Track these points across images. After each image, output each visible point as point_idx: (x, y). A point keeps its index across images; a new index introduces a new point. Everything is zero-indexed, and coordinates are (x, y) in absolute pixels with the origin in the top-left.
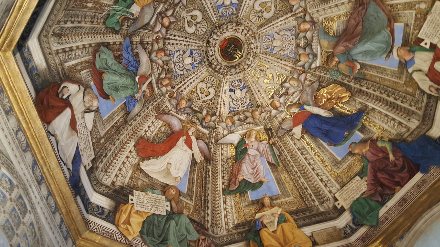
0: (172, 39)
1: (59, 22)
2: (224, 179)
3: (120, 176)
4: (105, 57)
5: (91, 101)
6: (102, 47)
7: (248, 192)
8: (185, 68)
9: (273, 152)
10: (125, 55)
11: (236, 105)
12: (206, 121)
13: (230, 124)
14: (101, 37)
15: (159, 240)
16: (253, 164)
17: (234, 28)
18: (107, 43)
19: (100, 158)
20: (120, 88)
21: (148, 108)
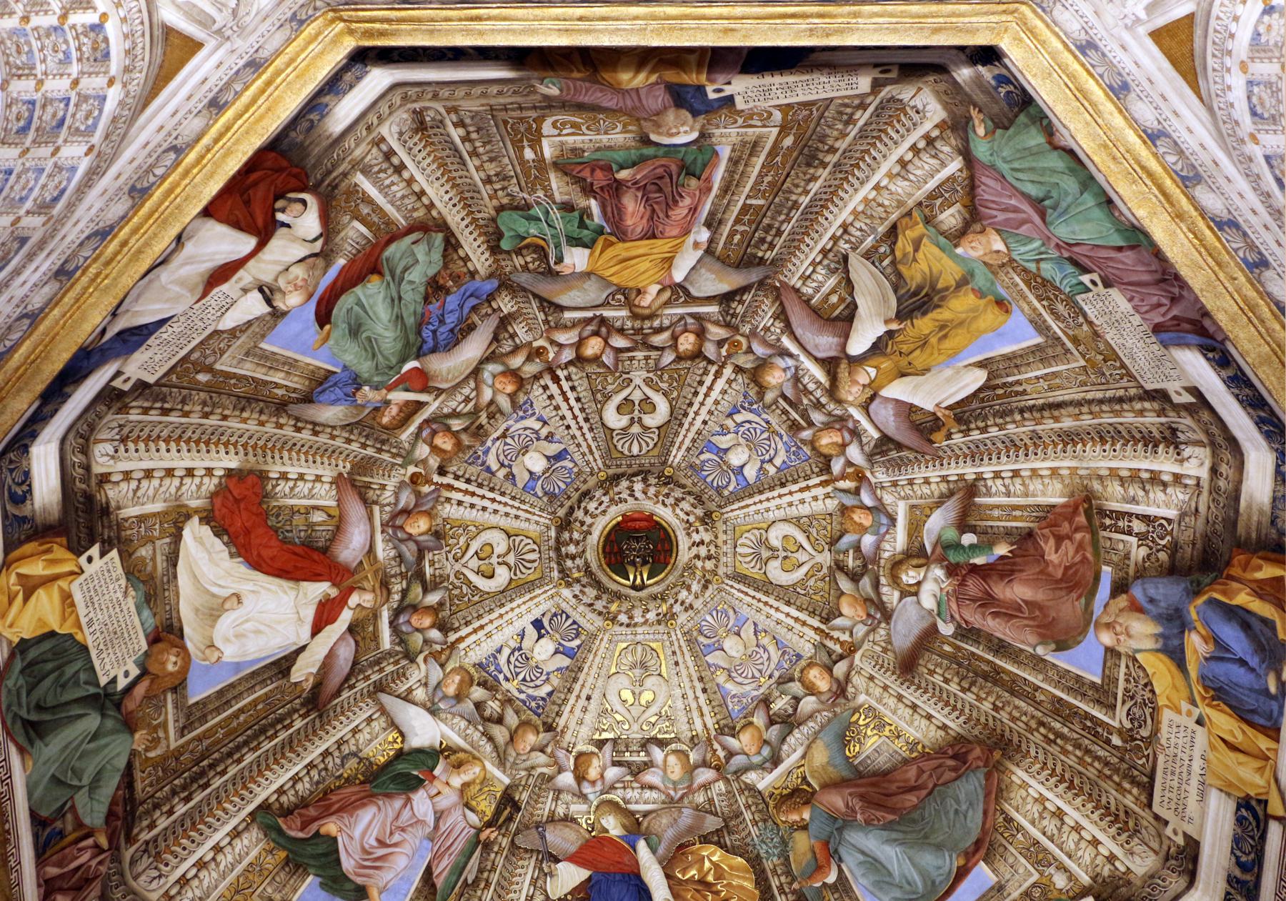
0: (560, 388)
1: (454, 110)
2: (293, 786)
3: (134, 484)
4: (421, 257)
6: (440, 236)
7: (311, 878)
8: (510, 466)
9: (463, 860)
10: (452, 301)
11: (512, 667)
12: (413, 621)
13: (451, 690)
14: (463, 219)
15: (28, 712)
16: (391, 833)
17: (692, 519)
18: (457, 241)
19: (155, 401)
20: (364, 335)
21: (349, 441)
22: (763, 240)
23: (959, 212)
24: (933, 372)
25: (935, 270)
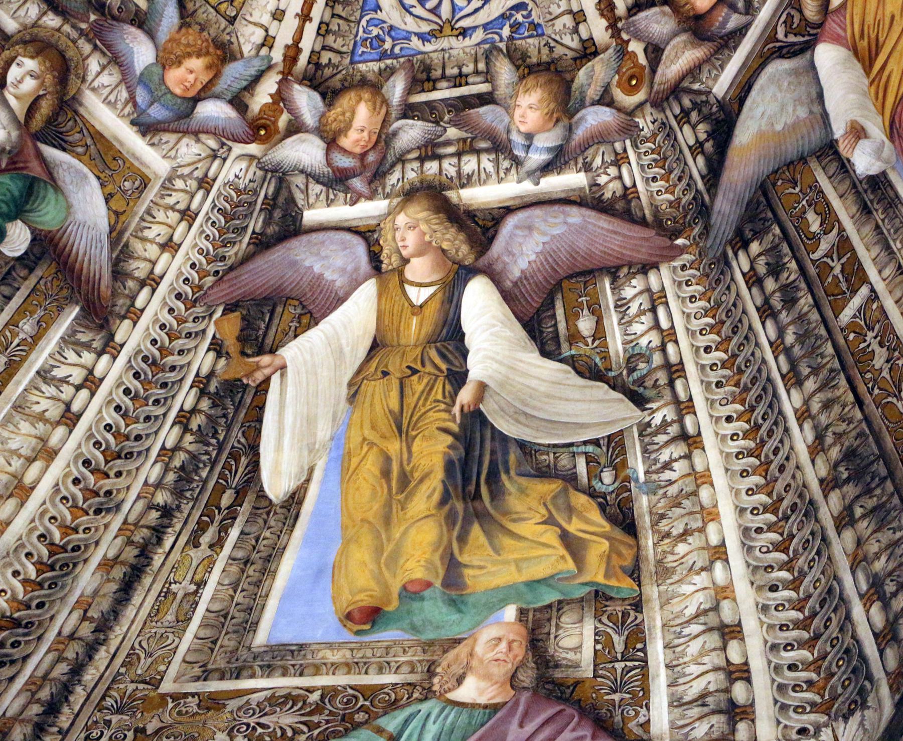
22: (775, 270)
23: (577, 666)
24: (343, 405)
25: (507, 541)
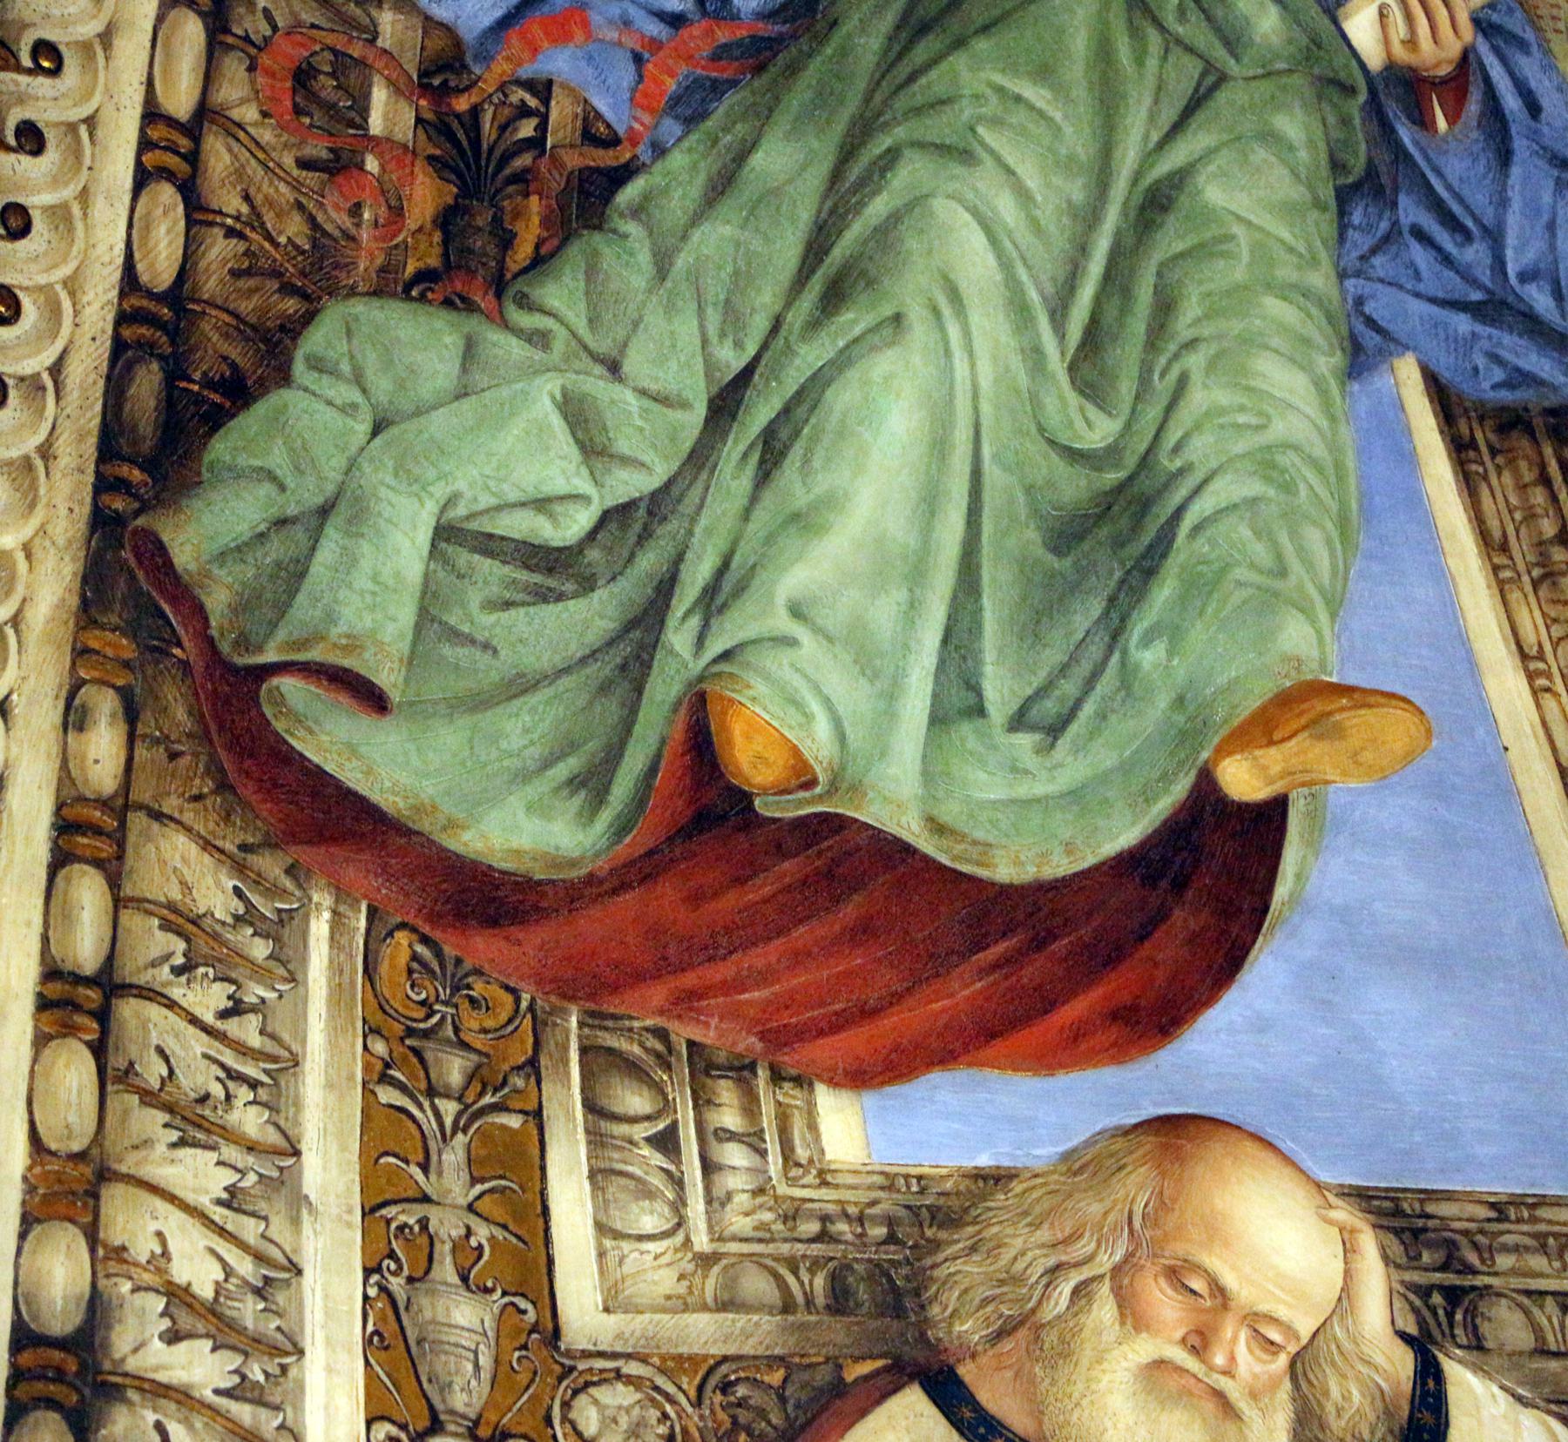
5: (1200, 1342)
20: (1099, 431)
